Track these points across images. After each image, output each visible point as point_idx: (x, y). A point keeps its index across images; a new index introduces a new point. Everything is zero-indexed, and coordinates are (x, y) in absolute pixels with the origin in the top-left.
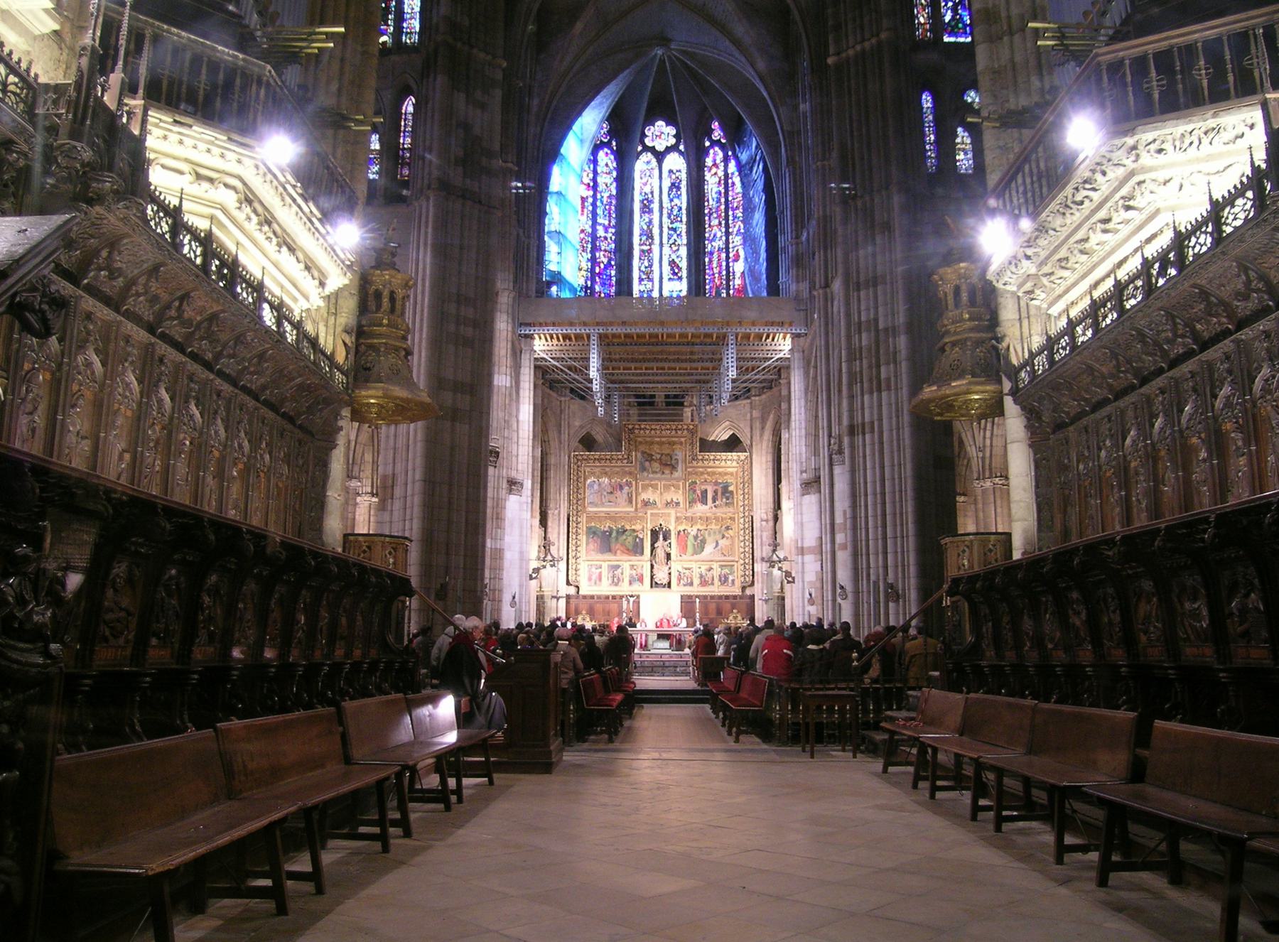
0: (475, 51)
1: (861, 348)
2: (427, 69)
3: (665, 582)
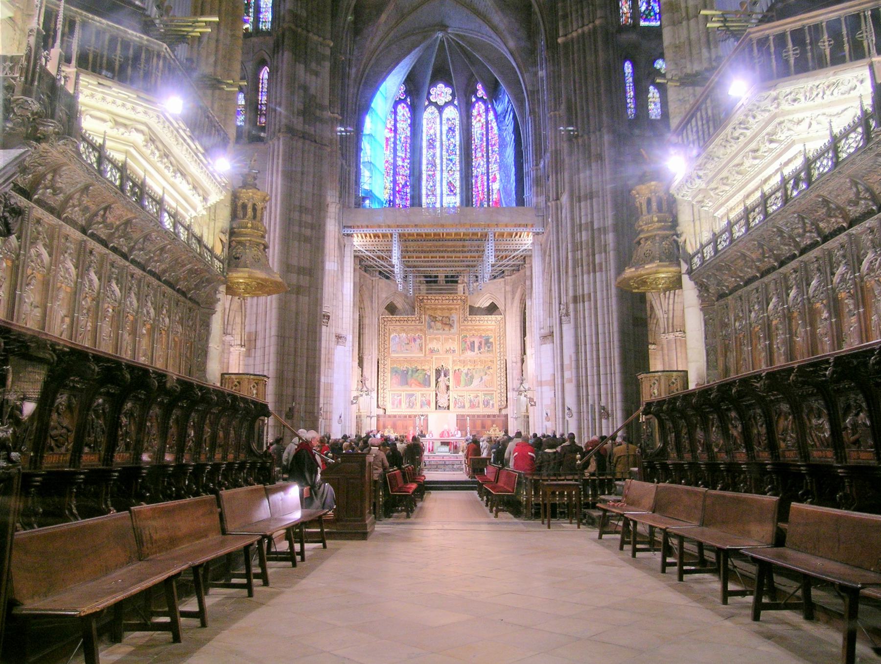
0: (311, 35)
1: (581, 242)
2: (277, 47)
3: (446, 405)
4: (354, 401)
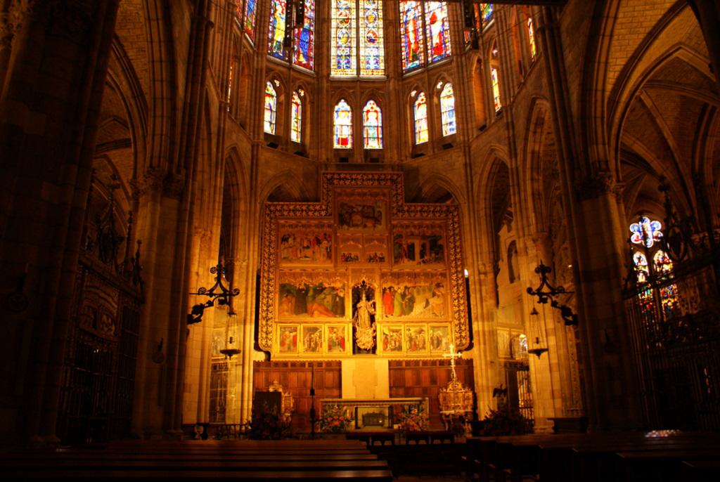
3: (369, 346)
4: (195, 316)
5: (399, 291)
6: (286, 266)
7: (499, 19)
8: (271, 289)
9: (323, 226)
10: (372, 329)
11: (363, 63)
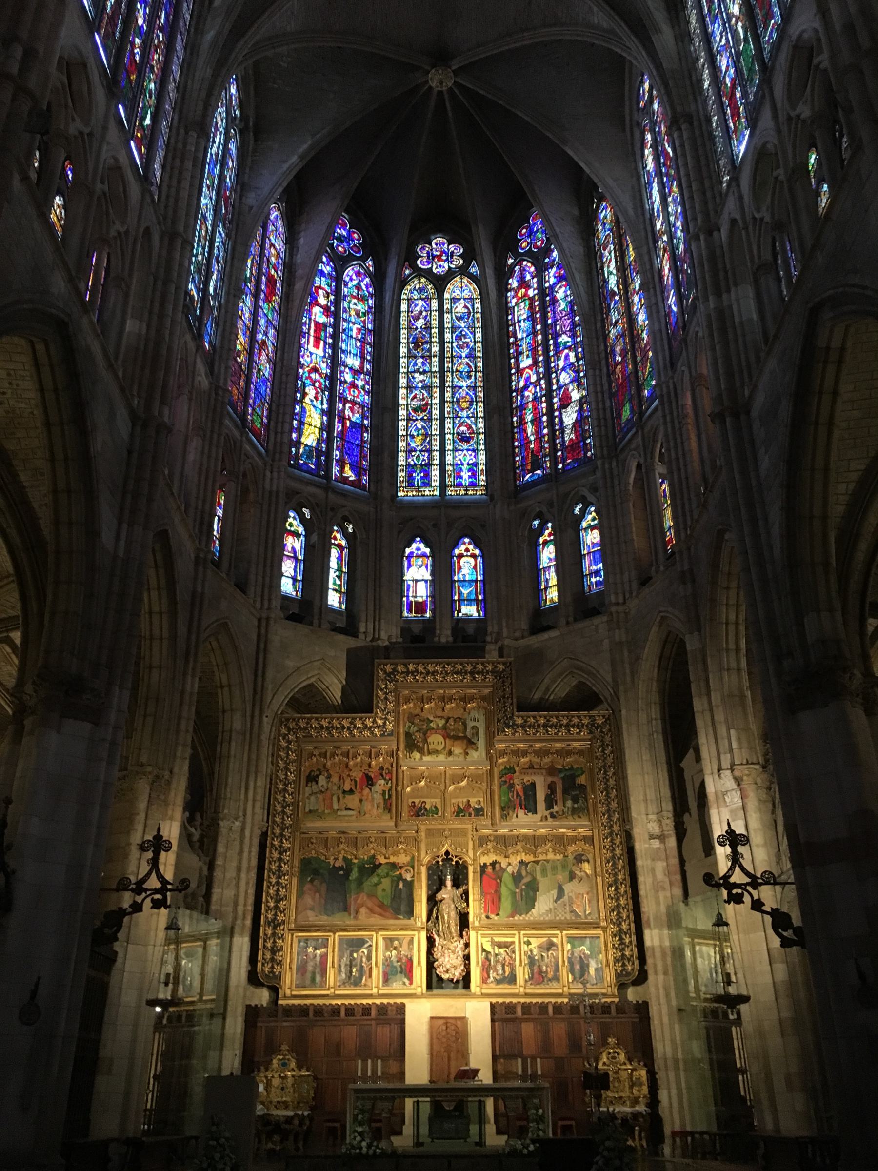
3: (457, 974)
5: (510, 870)
6: (313, 825)
7: (666, 399)
8: (285, 868)
9: (378, 755)
10: (462, 942)
11: (450, 476)
